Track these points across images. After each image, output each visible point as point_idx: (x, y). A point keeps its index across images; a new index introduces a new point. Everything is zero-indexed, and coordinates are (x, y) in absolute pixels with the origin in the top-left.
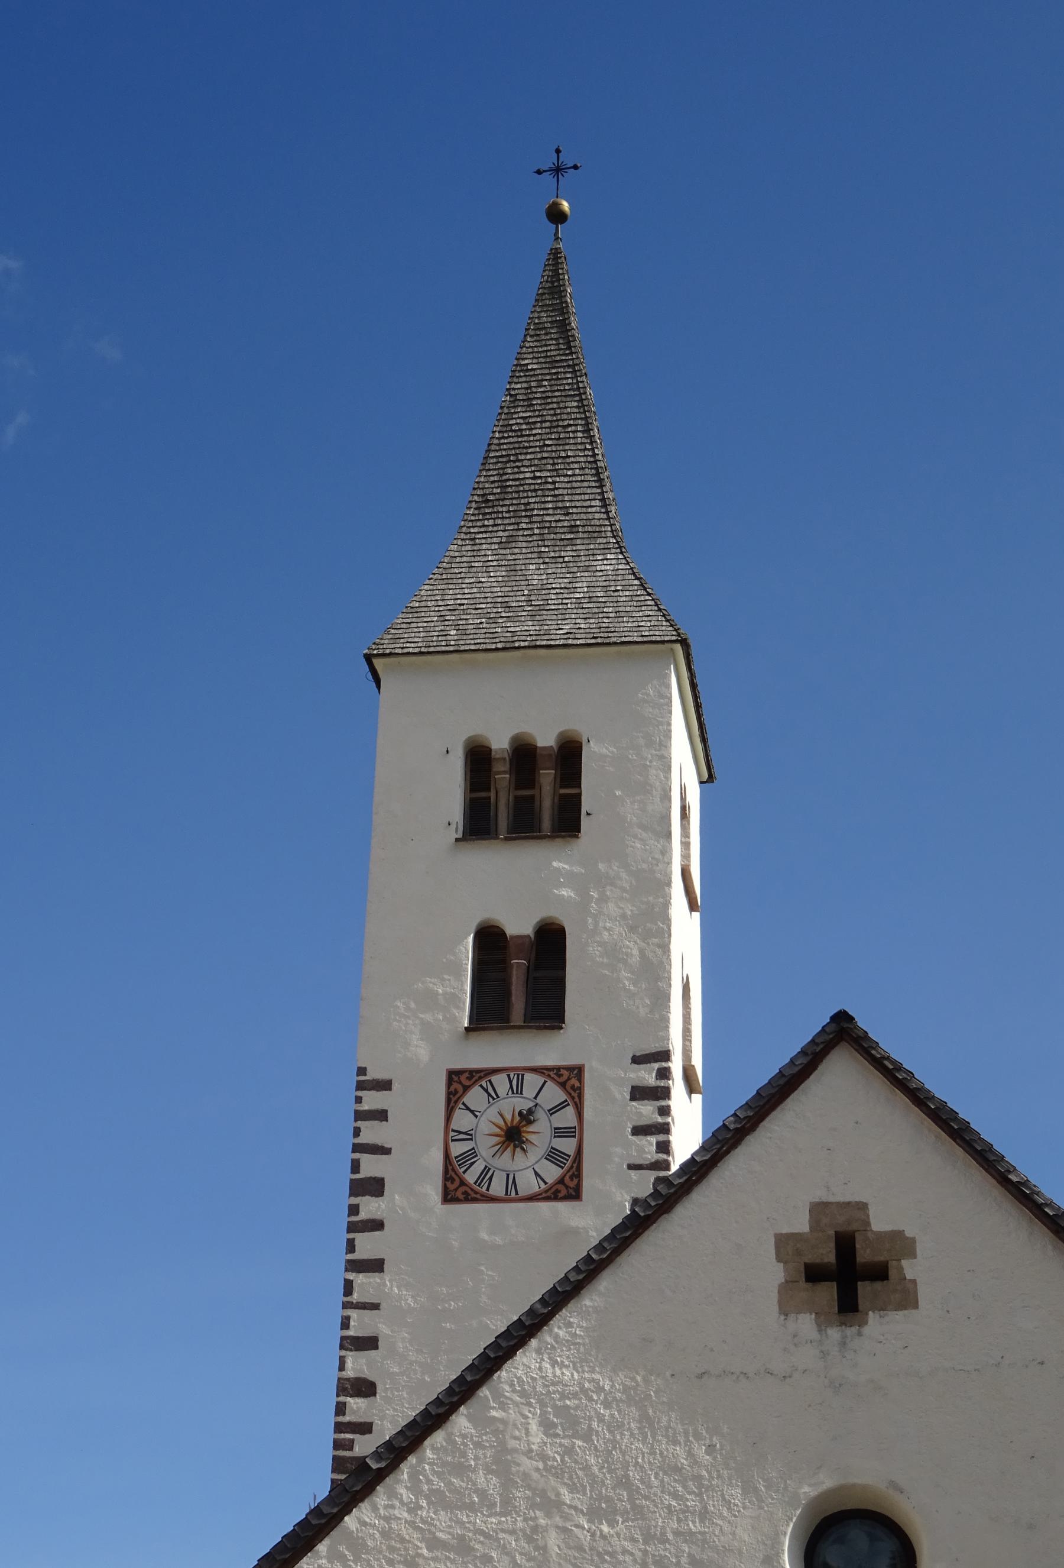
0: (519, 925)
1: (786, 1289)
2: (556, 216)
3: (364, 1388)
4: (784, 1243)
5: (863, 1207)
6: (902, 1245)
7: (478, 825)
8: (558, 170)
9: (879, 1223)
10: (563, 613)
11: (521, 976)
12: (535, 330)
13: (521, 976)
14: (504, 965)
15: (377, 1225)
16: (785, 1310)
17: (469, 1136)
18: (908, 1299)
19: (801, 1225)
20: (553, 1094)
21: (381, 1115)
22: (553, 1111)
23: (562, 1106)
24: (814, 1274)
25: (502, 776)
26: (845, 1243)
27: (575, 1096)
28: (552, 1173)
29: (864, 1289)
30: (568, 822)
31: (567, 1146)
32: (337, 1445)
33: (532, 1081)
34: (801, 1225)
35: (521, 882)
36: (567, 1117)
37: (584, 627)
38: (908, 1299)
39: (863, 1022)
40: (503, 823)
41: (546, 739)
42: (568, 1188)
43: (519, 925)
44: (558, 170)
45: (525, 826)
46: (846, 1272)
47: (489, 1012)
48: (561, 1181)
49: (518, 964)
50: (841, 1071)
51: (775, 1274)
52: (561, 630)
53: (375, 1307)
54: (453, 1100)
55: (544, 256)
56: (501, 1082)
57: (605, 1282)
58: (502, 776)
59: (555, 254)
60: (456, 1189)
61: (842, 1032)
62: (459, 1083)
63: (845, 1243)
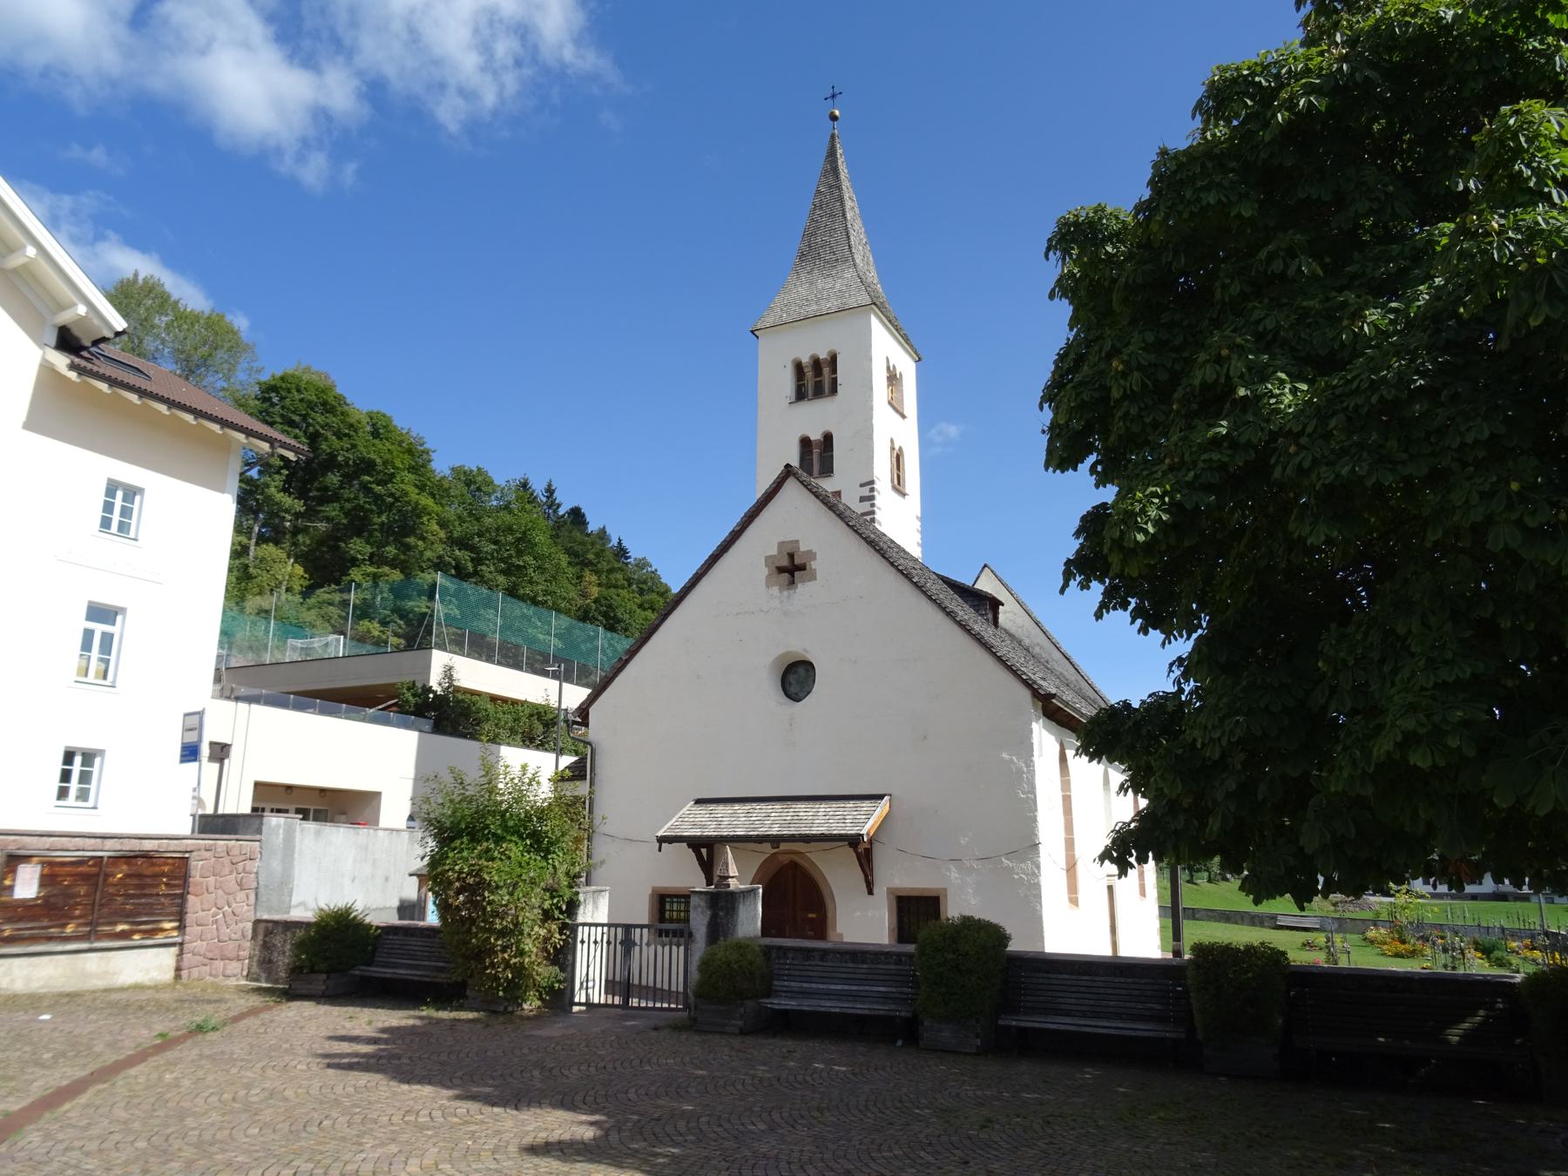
0: (816, 436)
1: (769, 577)
2: (834, 118)
6: (811, 555)
7: (800, 395)
8: (833, 96)
9: (803, 548)
10: (828, 300)
12: (825, 174)
13: (817, 455)
16: (768, 586)
18: (813, 577)
19: (774, 552)
24: (781, 570)
25: (809, 374)
29: (797, 574)
30: (834, 390)
34: (774, 552)
35: (814, 419)
37: (833, 304)
38: (813, 577)
40: (810, 392)
41: (823, 355)
43: (816, 436)
44: (833, 96)
45: (819, 392)
46: (791, 568)
49: (816, 451)
51: (765, 571)
52: (826, 306)
55: (828, 138)
57: (704, 582)
58: (809, 374)
59: (833, 136)
63: (791, 556)
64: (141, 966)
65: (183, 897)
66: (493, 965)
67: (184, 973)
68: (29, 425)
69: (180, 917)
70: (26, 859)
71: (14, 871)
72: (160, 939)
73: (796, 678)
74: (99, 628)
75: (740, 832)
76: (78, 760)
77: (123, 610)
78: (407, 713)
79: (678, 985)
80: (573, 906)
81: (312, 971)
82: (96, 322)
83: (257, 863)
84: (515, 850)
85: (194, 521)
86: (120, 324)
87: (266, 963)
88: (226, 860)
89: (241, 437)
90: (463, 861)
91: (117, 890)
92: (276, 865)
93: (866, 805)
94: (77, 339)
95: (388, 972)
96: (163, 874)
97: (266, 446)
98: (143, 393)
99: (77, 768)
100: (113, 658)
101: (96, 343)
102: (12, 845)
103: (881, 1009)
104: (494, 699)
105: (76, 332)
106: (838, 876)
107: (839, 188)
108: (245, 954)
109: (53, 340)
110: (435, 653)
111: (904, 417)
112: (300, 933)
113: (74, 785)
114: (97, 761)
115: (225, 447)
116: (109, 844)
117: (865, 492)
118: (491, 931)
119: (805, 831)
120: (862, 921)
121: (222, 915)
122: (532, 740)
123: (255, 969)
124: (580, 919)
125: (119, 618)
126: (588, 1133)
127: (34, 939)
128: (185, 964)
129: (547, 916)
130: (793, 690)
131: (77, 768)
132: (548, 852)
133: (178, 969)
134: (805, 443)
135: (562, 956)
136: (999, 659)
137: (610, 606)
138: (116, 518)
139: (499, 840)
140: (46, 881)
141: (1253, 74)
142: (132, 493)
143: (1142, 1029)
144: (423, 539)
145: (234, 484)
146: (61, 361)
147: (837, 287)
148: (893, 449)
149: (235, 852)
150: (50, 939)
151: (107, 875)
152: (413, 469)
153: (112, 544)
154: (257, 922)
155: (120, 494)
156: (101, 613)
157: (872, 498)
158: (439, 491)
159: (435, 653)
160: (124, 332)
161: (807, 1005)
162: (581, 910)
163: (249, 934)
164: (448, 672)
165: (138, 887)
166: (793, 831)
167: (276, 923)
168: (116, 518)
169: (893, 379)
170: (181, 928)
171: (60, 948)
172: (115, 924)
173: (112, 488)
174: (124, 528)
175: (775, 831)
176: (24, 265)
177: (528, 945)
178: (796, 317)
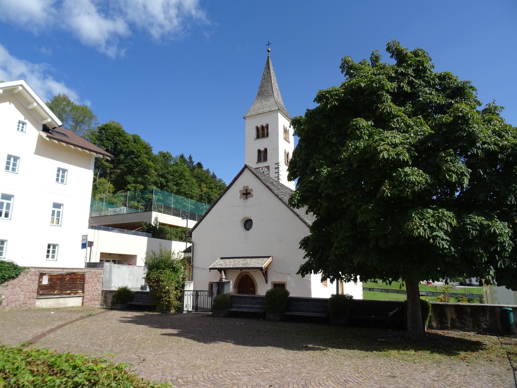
0: (262, 149)
2: (269, 51)
6: (252, 190)
7: (258, 137)
9: (250, 188)
11: (262, 155)
12: (266, 68)
13: (262, 155)
18: (252, 196)
19: (242, 189)
20: (266, 169)
24: (244, 194)
25: (260, 131)
27: (269, 169)
30: (268, 136)
33: (264, 168)
34: (242, 189)
35: (262, 144)
37: (267, 109)
38: (252, 196)
41: (264, 125)
43: (262, 149)
46: (246, 194)
47: (259, 160)
51: (239, 195)
58: (260, 131)
59: (268, 57)
61: (246, 167)
63: (246, 190)
64: (73, 302)
65: (83, 284)
66: (162, 301)
67: (84, 304)
68: (36, 153)
69: (83, 289)
70: (45, 274)
71: (42, 277)
72: (78, 295)
73: (248, 224)
74: (56, 210)
75: (231, 267)
76: (51, 247)
77: (63, 205)
78: (144, 232)
79: (209, 307)
80: (183, 286)
81: (117, 303)
82: (54, 123)
83: (102, 275)
84: (168, 271)
85: (82, 178)
86: (60, 123)
87: (105, 301)
88: (94, 275)
89: (95, 154)
90: (154, 275)
91: (66, 282)
92: (107, 276)
93: (265, 259)
94: (48, 128)
95: (136, 303)
96: (78, 278)
97: (102, 156)
98: (67, 143)
99: (51, 249)
100: (60, 218)
101: (53, 128)
102: (42, 271)
103: (257, 311)
104: (171, 226)
105: (48, 126)
106: (258, 279)
107: (270, 73)
108: (100, 299)
109: (41, 129)
110: (153, 212)
111: (289, 142)
112: (114, 294)
113: (51, 254)
114: (57, 247)
115: (90, 156)
116: (65, 270)
117: (276, 166)
118: (162, 292)
119: (248, 266)
120: (263, 289)
121: (94, 289)
122: (182, 239)
123: (102, 303)
124: (185, 289)
125: (62, 207)
126: (176, 332)
127: (47, 295)
128: (84, 301)
129: (176, 288)
130: (247, 227)
131: (51, 249)
132: (177, 272)
133: (83, 303)
134: (259, 151)
135: (181, 299)
136: (301, 219)
137: (209, 195)
138: (60, 178)
139: (164, 269)
140: (50, 280)
141: (326, 94)
142: (64, 171)
143: (318, 315)
144: (149, 175)
145: (93, 166)
146: (44, 135)
147: (267, 104)
148: (285, 152)
149: (97, 272)
150: (51, 294)
151: (65, 279)
152: (146, 153)
153: (59, 185)
154: (103, 291)
155: (61, 171)
156: (57, 205)
157: (278, 168)
158: (154, 160)
159: (153, 212)
160: (61, 126)
161: (239, 310)
162: (185, 287)
163: (101, 294)
164: (156, 219)
165: (72, 281)
166: (245, 266)
167: (108, 291)
168: (60, 178)
169: (286, 131)
170: (83, 292)
171: (53, 297)
172: (67, 291)
173: (59, 170)
174: (62, 181)
175: (240, 266)
176: (34, 108)
177: (171, 296)
178: (256, 113)
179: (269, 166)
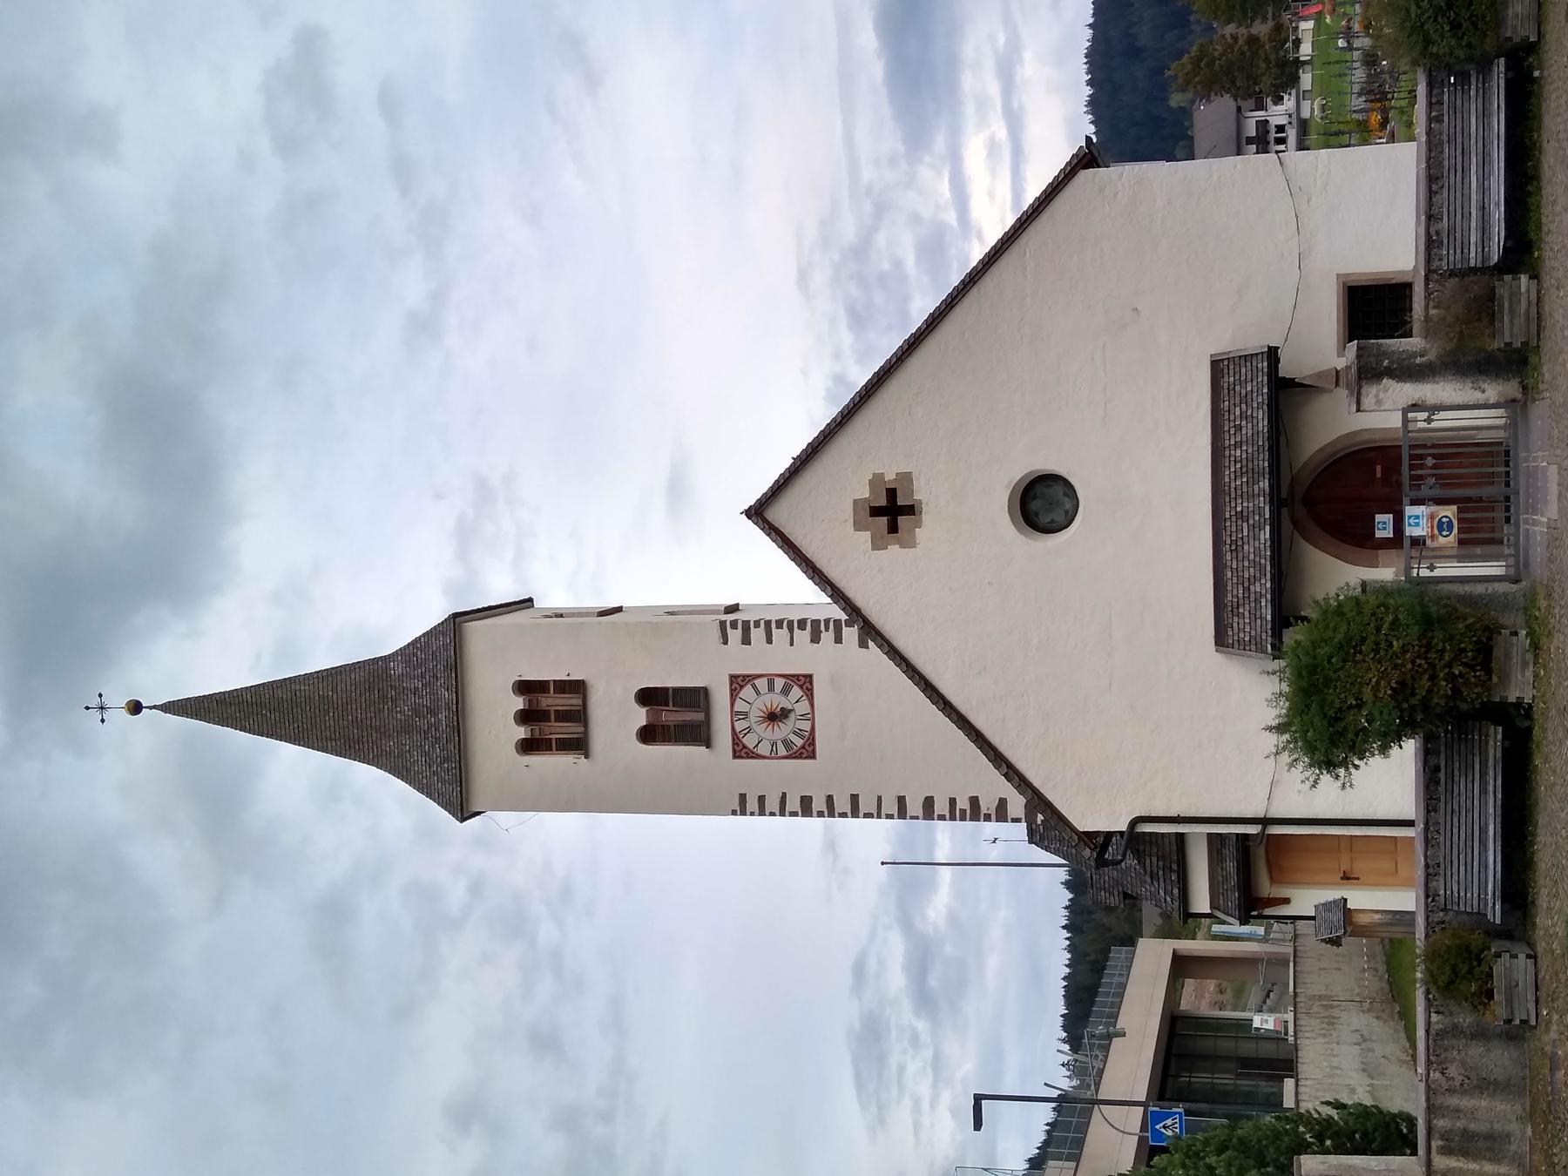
0: (640, 716)
3: (929, 804)
4: (877, 545)
5: (855, 502)
6: (876, 480)
13: (674, 715)
14: (665, 728)
15: (830, 799)
16: (913, 545)
17: (774, 744)
18: (906, 478)
19: (866, 536)
21: (761, 799)
22: (758, 693)
23: (754, 687)
24: (893, 528)
26: (876, 512)
27: (748, 679)
28: (796, 692)
30: (577, 687)
31: (779, 683)
32: (963, 819)
33: (740, 706)
34: (866, 536)
35: (615, 719)
36: (762, 684)
38: (906, 478)
39: (751, 500)
41: (519, 703)
42: (805, 682)
43: (640, 716)
46: (892, 511)
47: (699, 734)
48: (801, 687)
50: (776, 514)
51: (894, 549)
53: (880, 798)
54: (751, 755)
56: (739, 726)
60: (808, 750)
61: (757, 513)
62: (740, 751)
63: (876, 512)
73: (1043, 503)
134: (648, 735)
179: (733, 678)
